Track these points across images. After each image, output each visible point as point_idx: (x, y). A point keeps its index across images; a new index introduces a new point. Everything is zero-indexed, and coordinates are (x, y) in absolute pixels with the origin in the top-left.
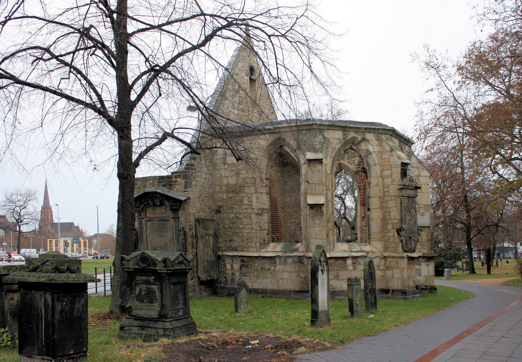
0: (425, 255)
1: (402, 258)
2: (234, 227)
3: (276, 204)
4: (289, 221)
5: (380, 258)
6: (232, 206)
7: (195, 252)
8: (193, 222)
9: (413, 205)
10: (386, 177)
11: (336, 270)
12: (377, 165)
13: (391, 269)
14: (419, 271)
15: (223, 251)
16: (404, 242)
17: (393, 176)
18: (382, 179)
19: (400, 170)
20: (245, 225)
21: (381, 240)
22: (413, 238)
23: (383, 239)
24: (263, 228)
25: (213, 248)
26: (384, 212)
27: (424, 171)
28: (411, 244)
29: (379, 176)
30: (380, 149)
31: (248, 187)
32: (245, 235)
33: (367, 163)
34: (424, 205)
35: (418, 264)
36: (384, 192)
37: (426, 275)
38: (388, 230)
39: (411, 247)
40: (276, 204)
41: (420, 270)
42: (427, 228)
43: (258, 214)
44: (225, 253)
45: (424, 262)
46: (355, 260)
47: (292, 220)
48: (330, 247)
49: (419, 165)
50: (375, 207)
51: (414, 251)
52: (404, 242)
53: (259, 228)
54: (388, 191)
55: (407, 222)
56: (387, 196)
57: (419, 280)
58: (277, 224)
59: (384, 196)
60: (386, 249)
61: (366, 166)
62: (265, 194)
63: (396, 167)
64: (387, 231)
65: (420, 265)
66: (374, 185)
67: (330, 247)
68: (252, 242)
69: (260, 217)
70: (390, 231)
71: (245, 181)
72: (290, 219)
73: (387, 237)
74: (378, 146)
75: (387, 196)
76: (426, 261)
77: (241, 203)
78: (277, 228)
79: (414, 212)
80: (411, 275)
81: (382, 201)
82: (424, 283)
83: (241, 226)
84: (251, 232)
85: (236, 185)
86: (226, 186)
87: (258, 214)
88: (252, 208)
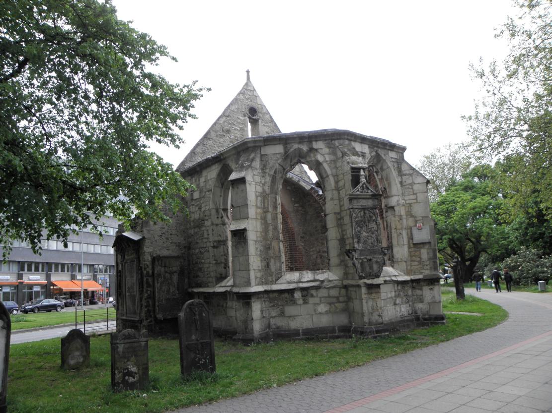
0: (427, 278)
3: (294, 234)
4: (312, 250)
5: (340, 288)
6: (197, 241)
7: (152, 290)
8: (148, 261)
9: (374, 218)
11: (281, 305)
16: (359, 266)
23: (343, 263)
24: (219, 261)
25: (178, 285)
27: (418, 177)
28: (371, 268)
29: (334, 188)
30: (332, 157)
32: (206, 270)
34: (422, 217)
35: (419, 289)
37: (430, 302)
39: (371, 271)
40: (294, 234)
41: (422, 295)
43: (214, 247)
44: (196, 290)
45: (426, 285)
46: (306, 292)
47: (314, 249)
48: (272, 278)
49: (411, 172)
50: (331, 226)
51: (378, 276)
53: (214, 262)
58: (295, 253)
62: (221, 226)
65: (421, 289)
66: (329, 199)
68: (210, 277)
69: (215, 250)
72: (312, 248)
74: (330, 154)
76: (429, 284)
78: (295, 258)
79: (375, 226)
81: (339, 217)
82: (427, 312)
85: (199, 219)
86: (194, 221)
87: (214, 247)
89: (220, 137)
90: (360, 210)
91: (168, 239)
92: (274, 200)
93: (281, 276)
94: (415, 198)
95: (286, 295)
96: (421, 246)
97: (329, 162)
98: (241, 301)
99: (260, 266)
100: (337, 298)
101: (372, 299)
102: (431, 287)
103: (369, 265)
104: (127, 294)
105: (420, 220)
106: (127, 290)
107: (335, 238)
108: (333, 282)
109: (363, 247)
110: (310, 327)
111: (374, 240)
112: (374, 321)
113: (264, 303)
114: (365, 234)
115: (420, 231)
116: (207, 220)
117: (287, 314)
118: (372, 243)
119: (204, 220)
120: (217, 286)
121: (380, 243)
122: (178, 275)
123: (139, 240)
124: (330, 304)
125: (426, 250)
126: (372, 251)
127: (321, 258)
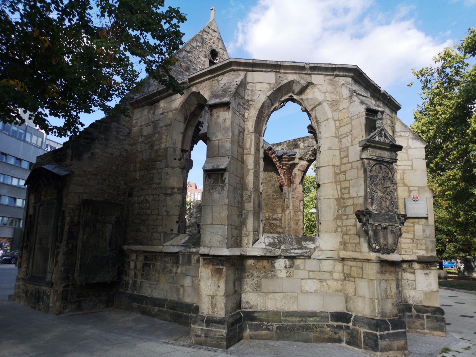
1: (368, 261)
2: (142, 213)
9: (390, 176)
10: (344, 135)
12: (331, 119)
13: (353, 279)
14: (414, 282)
15: (129, 244)
16: (371, 233)
17: (353, 131)
18: (338, 140)
19: (363, 121)
20: (152, 210)
21: (336, 231)
22: (390, 228)
23: (339, 230)
26: (341, 189)
28: (385, 238)
31: (159, 161)
33: (316, 117)
34: (418, 187)
35: (410, 272)
36: (341, 159)
37: (425, 289)
38: (348, 215)
39: (385, 243)
41: (415, 281)
42: (424, 221)
45: (421, 269)
51: (393, 251)
52: (371, 233)
53: (165, 213)
54: (347, 156)
55: (376, 202)
56: (345, 164)
57: (413, 297)
59: (342, 164)
60: (344, 244)
61: (315, 125)
63: (358, 118)
64: (346, 217)
66: (326, 149)
67: (248, 240)
70: (350, 217)
71: (157, 154)
73: (346, 226)
75: (345, 164)
76: (423, 267)
77: (151, 183)
80: (389, 293)
83: (148, 211)
84: (157, 219)
85: (149, 160)
88: (160, 188)
89: (178, 73)
90: (375, 163)
91: (105, 180)
92: (258, 142)
93: (258, 239)
94: (411, 164)
95: (265, 263)
96: (416, 220)
97: (329, 103)
98: (211, 267)
99: (237, 221)
100: (331, 273)
101: (386, 280)
102: (428, 271)
103: (383, 234)
104: (37, 246)
105: (415, 190)
106: (37, 240)
107: (331, 197)
108: (325, 252)
109: (377, 211)
110: (294, 310)
112: (388, 312)
113: (237, 272)
114: (380, 194)
115: (415, 202)
116: (161, 161)
117: (264, 289)
118: (387, 207)
119: (155, 161)
120: (165, 244)
121: (396, 208)
122: (112, 227)
123: (66, 176)
124: (320, 281)
125: (421, 226)
127: (270, 226)
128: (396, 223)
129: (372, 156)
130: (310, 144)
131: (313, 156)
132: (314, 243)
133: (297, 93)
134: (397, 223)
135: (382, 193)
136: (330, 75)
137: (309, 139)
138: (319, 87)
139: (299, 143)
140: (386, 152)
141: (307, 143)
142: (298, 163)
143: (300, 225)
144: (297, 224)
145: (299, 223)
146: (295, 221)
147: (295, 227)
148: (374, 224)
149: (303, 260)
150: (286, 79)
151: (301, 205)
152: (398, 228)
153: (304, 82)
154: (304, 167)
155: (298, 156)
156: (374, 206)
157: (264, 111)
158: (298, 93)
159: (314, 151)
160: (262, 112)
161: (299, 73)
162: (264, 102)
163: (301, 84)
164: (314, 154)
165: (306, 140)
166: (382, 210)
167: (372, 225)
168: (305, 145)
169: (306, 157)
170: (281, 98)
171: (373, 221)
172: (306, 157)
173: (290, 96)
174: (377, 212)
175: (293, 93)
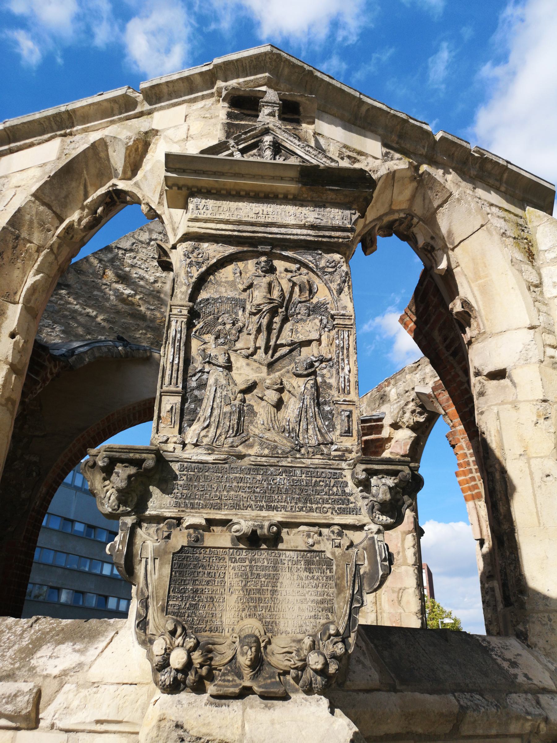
90: (231, 250)
103: (245, 577)
109: (211, 449)
111: (303, 411)
126: (282, 480)
128: (342, 512)
129: (206, 221)
130: (409, 386)
131: (421, 414)
132: (81, 652)
133: (124, 172)
134: (356, 511)
135: (258, 370)
136: (203, 98)
137: (406, 374)
138: (170, 133)
139: (388, 389)
140: (291, 209)
141: (402, 387)
142: (389, 439)
143: (408, 602)
144: (399, 602)
145: (404, 600)
146: (393, 592)
147: (392, 611)
148: (179, 521)
149: (10, 733)
150: (84, 143)
151: (406, 546)
152: (357, 537)
153: (129, 134)
154: (405, 445)
155: (387, 422)
156: (191, 434)
157: (24, 234)
158: (129, 173)
159: (418, 401)
160: (17, 237)
161: (120, 120)
162: (19, 210)
163: (120, 140)
164: (420, 406)
165: (400, 380)
166: (251, 446)
167: (170, 526)
168: (398, 390)
169: (405, 420)
170: (86, 197)
171: (177, 505)
172: (405, 420)
173: (108, 188)
174: (210, 458)
175: (116, 177)
